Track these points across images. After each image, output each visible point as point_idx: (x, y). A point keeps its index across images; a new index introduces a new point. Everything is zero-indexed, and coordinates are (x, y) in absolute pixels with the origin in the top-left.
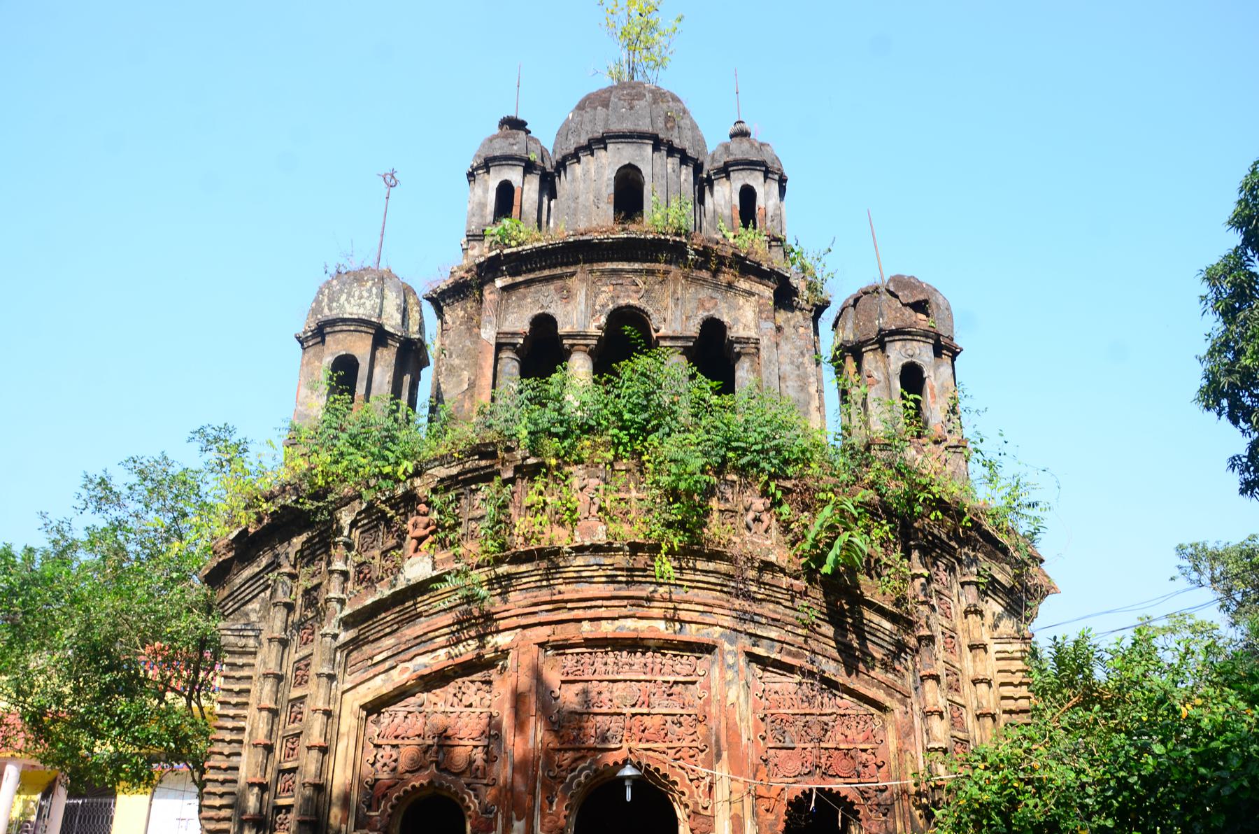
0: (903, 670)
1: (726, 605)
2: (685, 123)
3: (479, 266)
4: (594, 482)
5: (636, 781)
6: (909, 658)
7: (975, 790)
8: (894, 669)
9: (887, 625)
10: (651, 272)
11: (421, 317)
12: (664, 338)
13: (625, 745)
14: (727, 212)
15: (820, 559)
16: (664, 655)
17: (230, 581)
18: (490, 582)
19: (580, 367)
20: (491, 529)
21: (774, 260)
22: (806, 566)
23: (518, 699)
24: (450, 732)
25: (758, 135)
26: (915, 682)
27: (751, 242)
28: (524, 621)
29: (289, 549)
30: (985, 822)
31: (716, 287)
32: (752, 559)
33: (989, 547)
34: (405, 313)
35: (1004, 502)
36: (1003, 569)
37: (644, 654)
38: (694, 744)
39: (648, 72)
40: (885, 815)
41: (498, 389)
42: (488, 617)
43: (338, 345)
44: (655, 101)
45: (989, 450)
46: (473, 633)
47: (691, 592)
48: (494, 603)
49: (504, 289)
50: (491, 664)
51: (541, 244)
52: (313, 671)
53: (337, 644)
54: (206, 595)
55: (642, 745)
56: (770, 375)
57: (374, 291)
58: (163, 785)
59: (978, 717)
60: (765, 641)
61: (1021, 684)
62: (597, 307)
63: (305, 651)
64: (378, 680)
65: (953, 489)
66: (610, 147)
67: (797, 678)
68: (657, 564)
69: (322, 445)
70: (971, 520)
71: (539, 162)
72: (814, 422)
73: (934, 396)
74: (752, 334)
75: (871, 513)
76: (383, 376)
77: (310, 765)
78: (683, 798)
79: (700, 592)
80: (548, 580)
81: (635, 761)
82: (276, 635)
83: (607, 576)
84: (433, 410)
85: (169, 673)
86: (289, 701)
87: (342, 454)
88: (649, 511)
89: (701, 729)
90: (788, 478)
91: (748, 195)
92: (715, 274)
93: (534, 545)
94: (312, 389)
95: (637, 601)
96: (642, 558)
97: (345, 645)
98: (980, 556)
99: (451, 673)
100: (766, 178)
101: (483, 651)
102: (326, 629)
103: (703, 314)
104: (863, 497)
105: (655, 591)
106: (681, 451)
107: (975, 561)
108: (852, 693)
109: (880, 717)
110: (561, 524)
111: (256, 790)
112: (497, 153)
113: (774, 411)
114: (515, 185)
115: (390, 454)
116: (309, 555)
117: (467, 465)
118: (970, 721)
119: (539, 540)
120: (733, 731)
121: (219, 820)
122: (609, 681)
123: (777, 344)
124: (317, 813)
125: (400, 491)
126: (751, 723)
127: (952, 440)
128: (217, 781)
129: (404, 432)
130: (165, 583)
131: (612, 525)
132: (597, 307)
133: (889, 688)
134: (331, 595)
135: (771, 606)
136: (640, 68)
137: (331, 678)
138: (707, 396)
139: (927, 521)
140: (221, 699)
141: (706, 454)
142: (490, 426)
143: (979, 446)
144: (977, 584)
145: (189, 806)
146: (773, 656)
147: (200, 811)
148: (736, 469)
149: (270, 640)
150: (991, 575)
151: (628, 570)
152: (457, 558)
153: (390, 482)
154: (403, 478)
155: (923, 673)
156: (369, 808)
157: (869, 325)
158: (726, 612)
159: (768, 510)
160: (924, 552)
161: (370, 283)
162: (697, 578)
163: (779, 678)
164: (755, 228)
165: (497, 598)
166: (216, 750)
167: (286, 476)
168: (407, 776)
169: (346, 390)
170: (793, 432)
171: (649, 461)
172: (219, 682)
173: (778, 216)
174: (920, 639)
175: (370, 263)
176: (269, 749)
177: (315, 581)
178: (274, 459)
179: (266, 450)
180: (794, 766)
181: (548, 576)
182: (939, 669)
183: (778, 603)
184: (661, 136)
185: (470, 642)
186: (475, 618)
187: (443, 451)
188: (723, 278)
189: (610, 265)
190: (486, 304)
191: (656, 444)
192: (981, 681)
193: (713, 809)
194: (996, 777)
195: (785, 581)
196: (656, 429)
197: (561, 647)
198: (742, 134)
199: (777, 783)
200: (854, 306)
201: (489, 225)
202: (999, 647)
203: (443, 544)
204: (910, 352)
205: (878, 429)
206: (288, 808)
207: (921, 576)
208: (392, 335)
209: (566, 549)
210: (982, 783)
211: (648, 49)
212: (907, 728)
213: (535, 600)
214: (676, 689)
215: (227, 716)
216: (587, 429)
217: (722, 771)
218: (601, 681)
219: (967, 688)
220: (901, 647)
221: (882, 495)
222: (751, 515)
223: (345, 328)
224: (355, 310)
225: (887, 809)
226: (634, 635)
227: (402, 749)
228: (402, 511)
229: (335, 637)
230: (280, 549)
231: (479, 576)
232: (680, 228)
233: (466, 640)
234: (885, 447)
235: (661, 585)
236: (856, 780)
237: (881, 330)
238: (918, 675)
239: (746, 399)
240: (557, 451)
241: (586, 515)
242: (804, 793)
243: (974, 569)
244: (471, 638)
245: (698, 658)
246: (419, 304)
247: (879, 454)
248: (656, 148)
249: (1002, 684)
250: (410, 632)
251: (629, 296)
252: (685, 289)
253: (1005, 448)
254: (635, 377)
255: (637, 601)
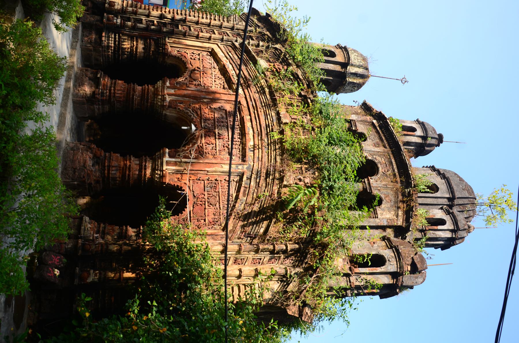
1: (263, 166)
9: (262, 230)
16: (240, 145)
42: (248, 86)
47: (266, 154)
63: (230, 34)
80: (265, 106)
83: (269, 124)
95: (260, 134)
97: (233, 44)
125: (290, 61)
135: (264, 185)
146: (243, 183)
158: (260, 167)
162: (272, 156)
181: (267, 106)
183: (266, 188)
186: (248, 83)
208: (346, 69)
227: (198, 61)
255: (260, 134)
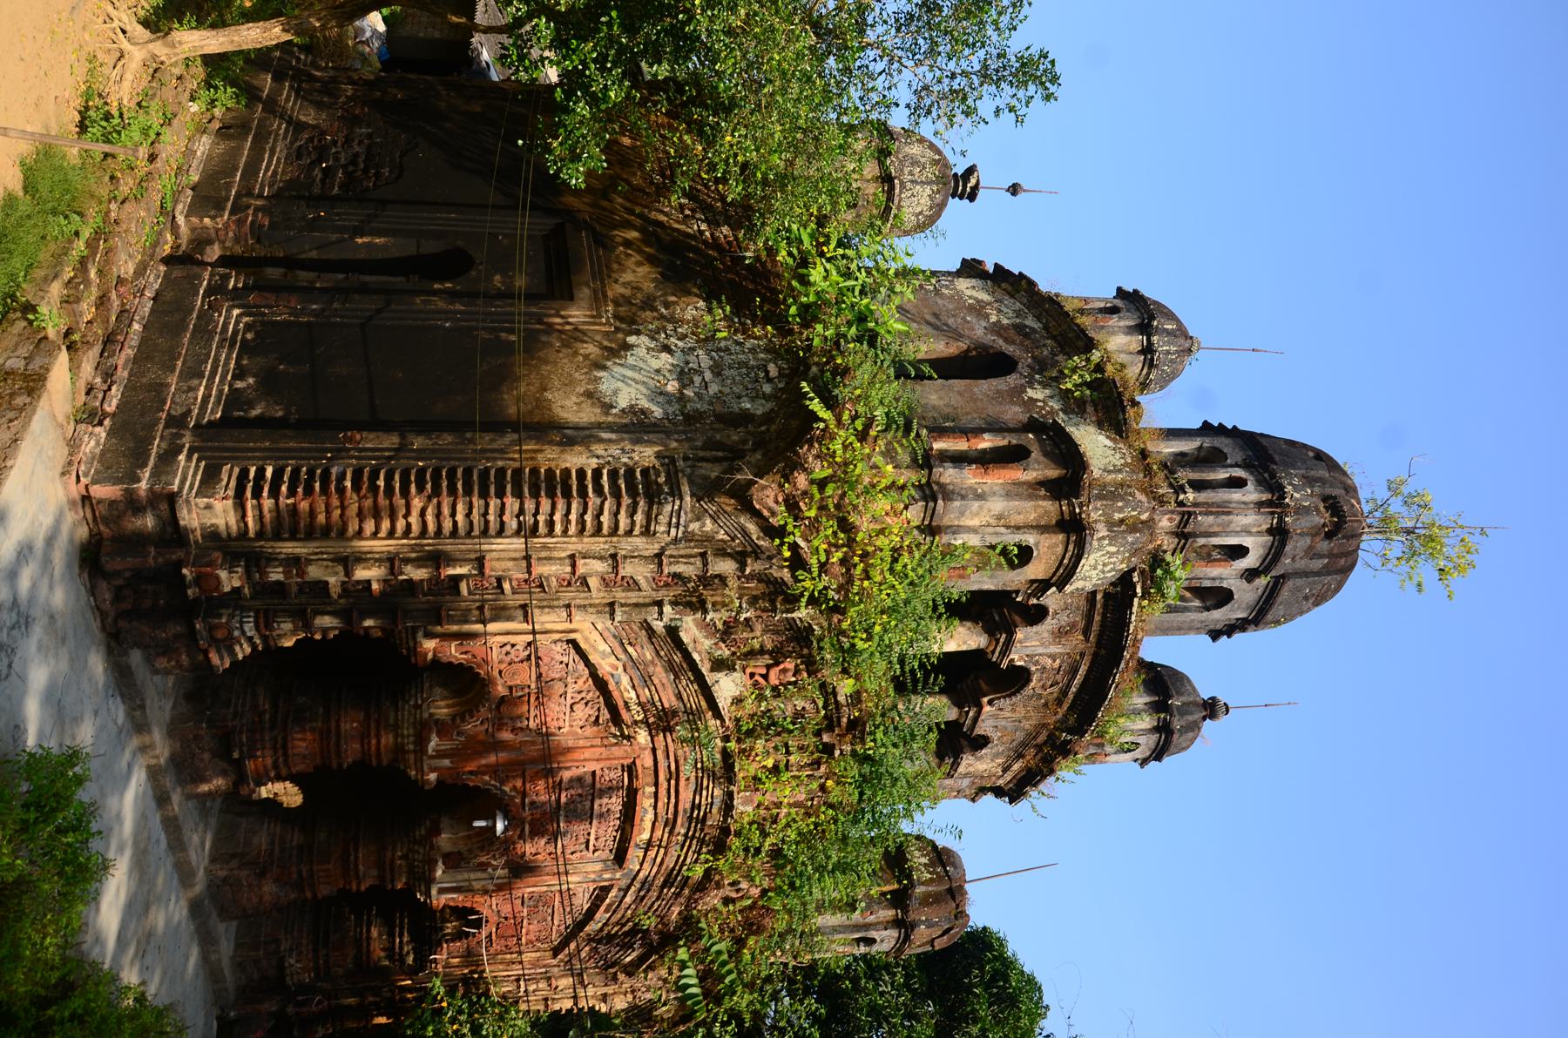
213: (681, 762)
226: (637, 821)
255: (671, 824)
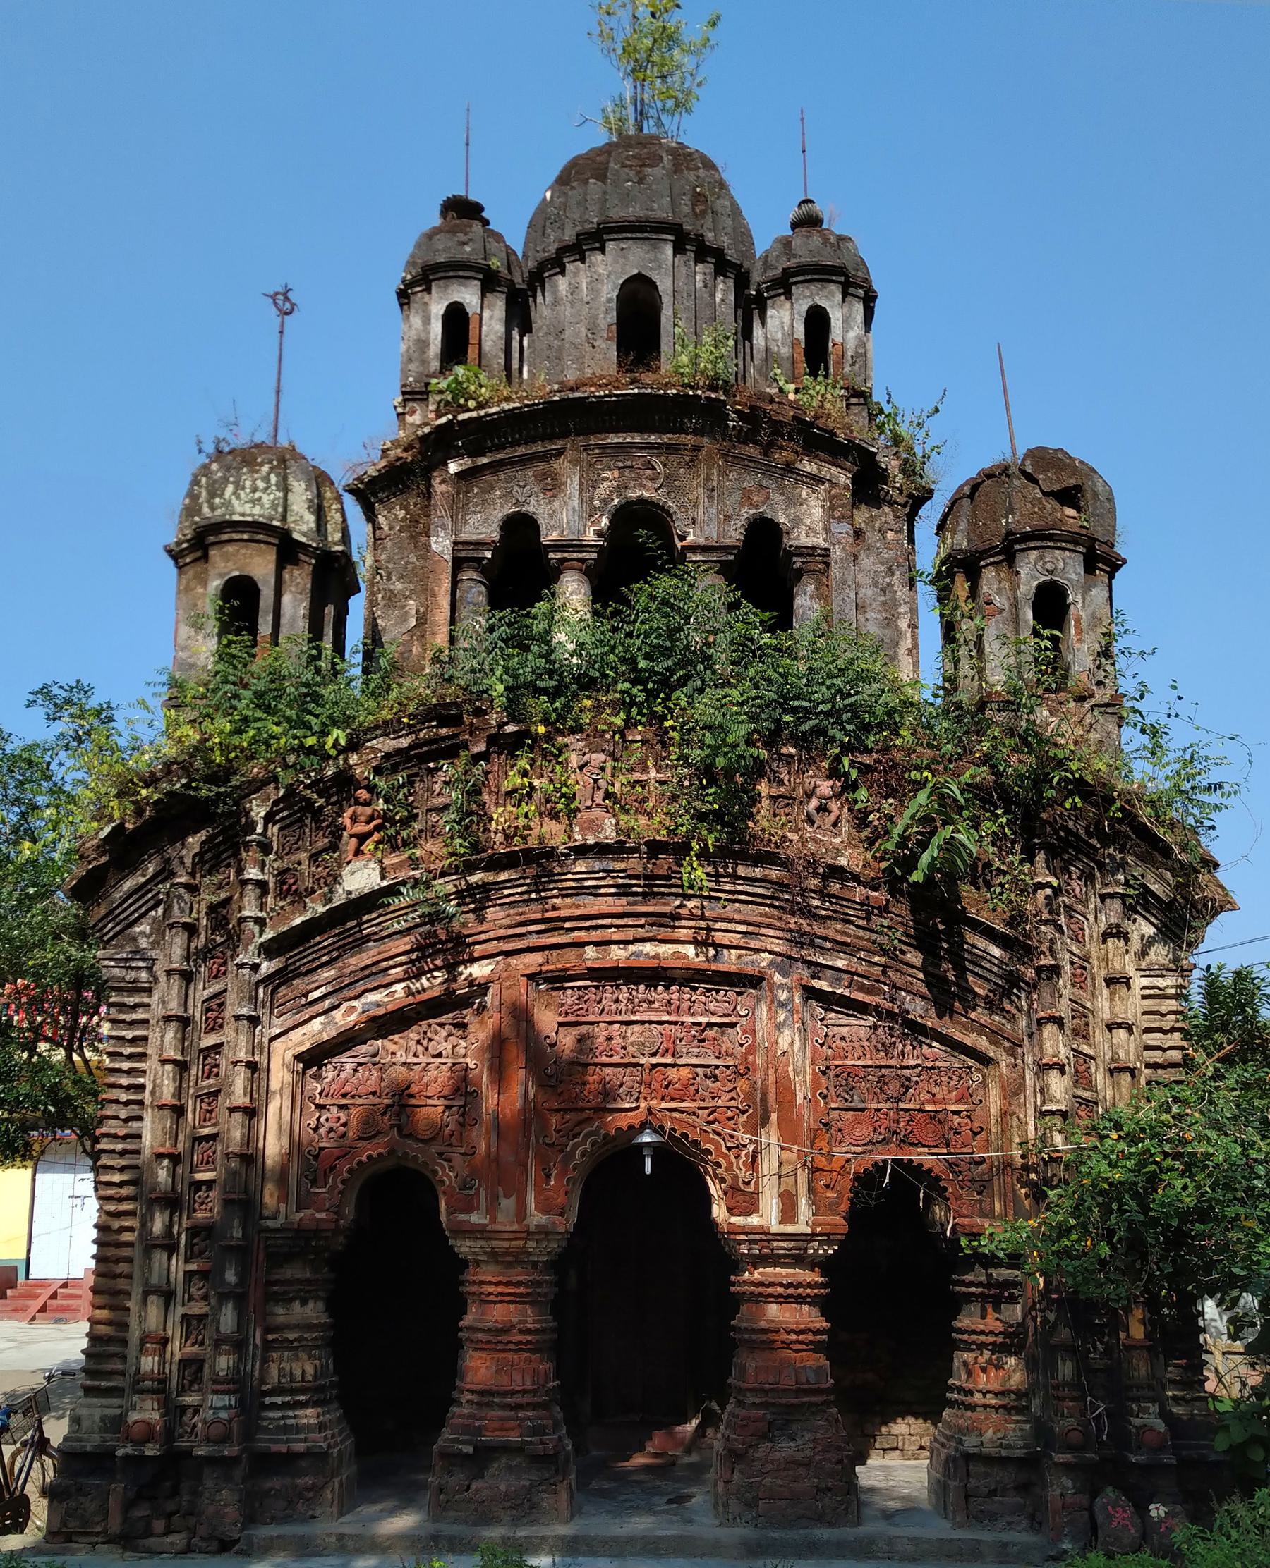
0: (1014, 1011)
2: (722, 204)
3: (423, 439)
4: (598, 758)
5: (656, 1149)
6: (1023, 995)
7: (1104, 1167)
8: (1003, 1009)
9: (997, 952)
10: (672, 449)
11: (344, 520)
12: (694, 548)
13: (643, 1105)
14: (785, 351)
15: (909, 863)
17: (107, 895)
18: (459, 894)
19: (573, 592)
20: (459, 823)
21: (856, 427)
22: (888, 871)
23: (497, 1048)
24: (414, 1089)
25: (836, 224)
26: (1029, 1026)
27: (820, 398)
28: (507, 946)
29: (184, 852)
30: (1114, 1206)
31: (768, 470)
32: (815, 864)
33: (1144, 846)
34: (320, 512)
35: (1168, 785)
36: (1161, 877)
37: (667, 988)
38: (733, 1103)
39: (665, 119)
40: (979, 1193)
41: (462, 625)
43: (228, 563)
44: (677, 169)
45: (1153, 709)
46: (438, 962)
47: (730, 907)
48: (466, 922)
49: (460, 475)
50: (465, 1002)
51: (512, 405)
52: (229, 1012)
53: (258, 977)
54: (76, 916)
55: (664, 1105)
56: (843, 602)
57: (273, 479)
58: (46, 1157)
59: (1112, 1072)
60: (829, 973)
61: (1173, 1030)
62: (597, 503)
63: (217, 987)
64: (316, 1024)
65: (1101, 765)
66: (610, 246)
67: (871, 1020)
68: (685, 870)
69: (217, 707)
70: (1122, 809)
71: (504, 271)
72: (906, 674)
73: (1079, 632)
74: (820, 541)
75: (982, 800)
76: (295, 608)
77: (235, 1131)
78: (719, 1171)
79: (743, 907)
80: (538, 892)
81: (656, 1124)
82: (175, 966)
84: (368, 656)
85: (39, 1019)
86: (201, 1051)
87: (245, 720)
88: (674, 798)
89: (742, 1084)
90: (868, 751)
91: (817, 321)
92: (767, 449)
93: (517, 845)
94: (198, 627)
95: (657, 919)
96: (665, 862)
98: (1130, 859)
99: (412, 1014)
100: (845, 294)
101: (454, 986)
102: (242, 958)
103: (748, 512)
104: (973, 777)
105: (682, 906)
106: (717, 709)
107: (1122, 865)
108: (945, 1040)
109: (979, 1070)
110: (555, 816)
111: (166, 1162)
112: (441, 259)
113: (849, 655)
114: (470, 311)
115: (314, 720)
116: (210, 860)
117: (421, 735)
118: (1100, 1078)
119: (524, 838)
120: (786, 1089)
121: (121, 1200)
122: (622, 1023)
123: (855, 557)
124: (246, 1191)
125: (330, 772)
126: (808, 1078)
127: (1102, 695)
128: (113, 1151)
129: (331, 688)
130: (19, 900)
131: (624, 818)
132: (597, 503)
133: (995, 1035)
134: (246, 913)
136: (652, 112)
137: (254, 1021)
138: (755, 634)
139: (1059, 810)
140: (111, 1050)
141: (753, 718)
142: (450, 680)
143: (1137, 706)
144: (1123, 897)
145: (84, 1183)
146: (839, 991)
147: (96, 1189)
148: (795, 740)
149: (169, 973)
150: (1143, 886)
151: (646, 877)
152: (414, 862)
153: (316, 759)
154: (333, 752)
155: (1041, 1014)
156: (314, 1182)
157: (992, 525)
158: (777, 933)
159: (837, 796)
160: (1053, 853)
161: (266, 468)
162: (740, 888)
163: (846, 1020)
164: (826, 376)
165: (471, 915)
166: (109, 1113)
167: (169, 750)
168: (360, 1144)
169: (245, 628)
170: (875, 686)
171: (673, 728)
172: (105, 1029)
173: (861, 357)
174: (1039, 970)
175: (262, 436)
176: (179, 1111)
177: (223, 895)
178: (151, 725)
179: (139, 714)
180: (863, 1132)
182: (1063, 1009)
183: (851, 923)
184: (686, 227)
185: (436, 974)
187: (386, 714)
188: (780, 457)
189: (613, 439)
190: (437, 500)
191: (683, 703)
192: (1119, 1026)
193: (757, 1184)
194: (1132, 1150)
195: (859, 892)
196: (683, 682)
197: (557, 980)
198: (808, 221)
199: (841, 1151)
200: (971, 496)
201: (433, 376)
202: (1145, 981)
203: (393, 844)
204: (1049, 566)
205: (997, 678)
206: (209, 1184)
207: (1048, 885)
209: (562, 849)
210: (1113, 1157)
211: (663, 77)
212: (1014, 1085)
213: (522, 918)
214: (711, 1033)
215: (119, 1071)
216: (587, 683)
217: (770, 1137)
218: (611, 1023)
219: (1099, 1035)
220: (1013, 980)
221: (998, 774)
222: (814, 803)
223: (235, 536)
224: (247, 508)
225: (983, 1186)
227: (353, 1111)
228: (334, 799)
229: (255, 968)
230: (171, 852)
231: (444, 886)
232: (716, 377)
233: (431, 971)
234: (1005, 706)
235: (689, 897)
236: (945, 1151)
237: (1009, 533)
238: (1034, 1017)
239: (811, 638)
240: (545, 713)
241: (589, 803)
242: (875, 1165)
243: (1121, 877)
244: (438, 969)
245: (739, 994)
246: (339, 499)
247: (998, 717)
248: (678, 249)
249: (1148, 1030)
250: (355, 961)
251: (642, 486)
252: (723, 473)
253: (1179, 707)
254: (653, 606)
255: (657, 919)
